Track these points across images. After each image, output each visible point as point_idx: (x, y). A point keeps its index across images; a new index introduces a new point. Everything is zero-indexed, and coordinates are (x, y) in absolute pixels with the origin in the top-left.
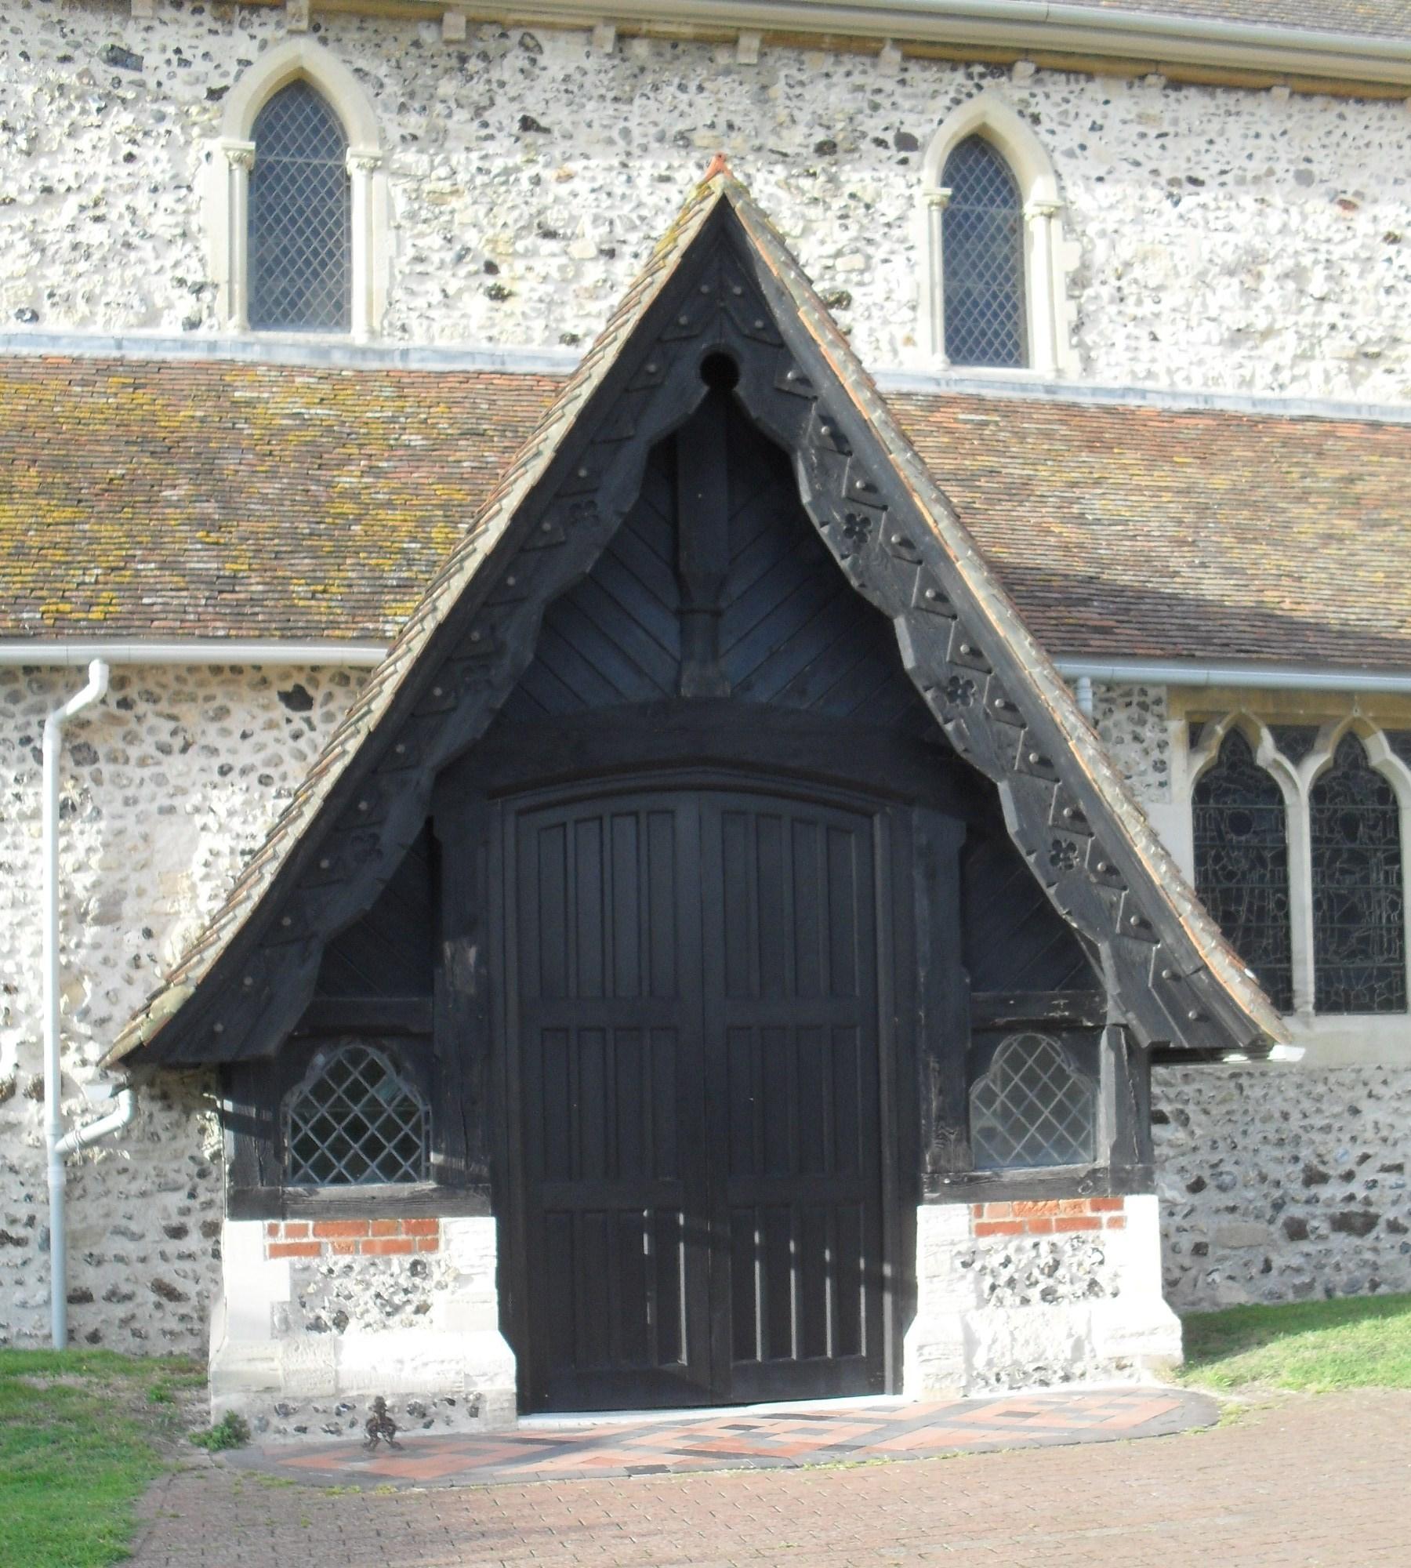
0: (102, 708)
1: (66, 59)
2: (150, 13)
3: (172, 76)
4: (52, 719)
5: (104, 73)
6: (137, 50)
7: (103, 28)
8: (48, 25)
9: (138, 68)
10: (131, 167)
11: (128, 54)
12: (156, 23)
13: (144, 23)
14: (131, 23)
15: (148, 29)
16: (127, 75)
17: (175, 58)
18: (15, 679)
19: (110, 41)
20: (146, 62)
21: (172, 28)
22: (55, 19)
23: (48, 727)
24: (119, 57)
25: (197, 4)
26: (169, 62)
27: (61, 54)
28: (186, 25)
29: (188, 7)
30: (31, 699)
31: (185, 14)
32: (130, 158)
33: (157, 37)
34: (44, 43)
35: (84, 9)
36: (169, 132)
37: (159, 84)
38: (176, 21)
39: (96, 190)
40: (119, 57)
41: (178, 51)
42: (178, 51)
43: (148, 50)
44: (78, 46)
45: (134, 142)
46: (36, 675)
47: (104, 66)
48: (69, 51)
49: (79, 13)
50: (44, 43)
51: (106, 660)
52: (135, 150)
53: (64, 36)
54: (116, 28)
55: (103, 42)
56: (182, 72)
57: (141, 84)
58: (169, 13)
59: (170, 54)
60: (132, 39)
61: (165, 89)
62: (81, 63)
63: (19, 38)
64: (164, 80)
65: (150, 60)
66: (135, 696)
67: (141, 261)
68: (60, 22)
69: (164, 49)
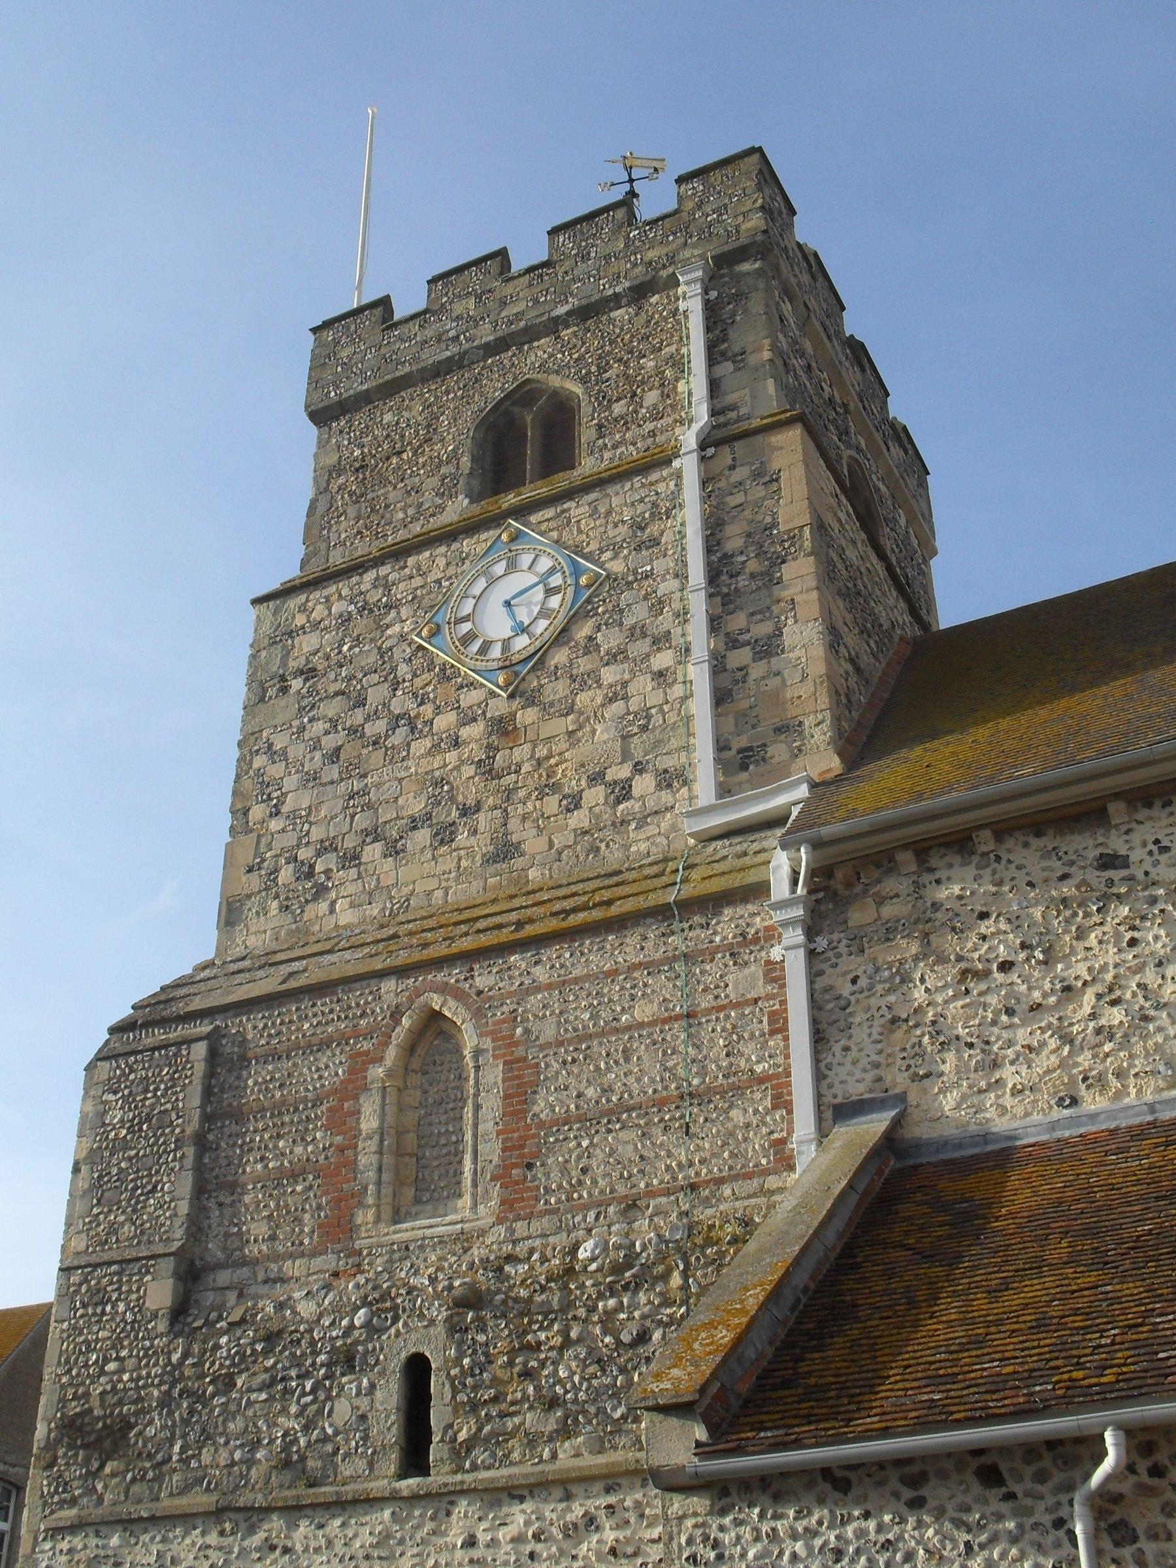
0: (1132, 1479)
1: (1064, 877)
2: (1127, 819)
3: (1156, 863)
4: (1078, 1497)
5: (1096, 878)
6: (1122, 852)
7: (1090, 843)
8: (1046, 855)
9: (1128, 867)
10: (1135, 950)
11: (1115, 856)
12: (1134, 825)
13: (1124, 828)
14: (1113, 831)
15: (1127, 832)
16: (1116, 875)
17: (1155, 848)
18: (1040, 1457)
19: (1097, 852)
20: (1131, 859)
21: (1149, 824)
22: (1050, 848)
23: (1077, 1507)
24: (1109, 862)
25: (1166, 798)
26: (1151, 853)
27: (1059, 874)
28: (1159, 819)
29: (1158, 803)
30: (1058, 1477)
31: (1156, 811)
32: (1133, 942)
33: (1136, 838)
35: (1072, 833)
36: (1162, 911)
37: (1147, 874)
38: (1150, 818)
39: (1109, 977)
40: (1109, 862)
41: (1157, 842)
42: (1157, 842)
43: (1131, 849)
44: (1072, 863)
45: (1133, 928)
46: (1060, 1449)
47: (1098, 873)
48: (1066, 870)
49: (1069, 838)
51: (1119, 1427)
52: (1136, 934)
53: (1060, 859)
54: (1101, 840)
55: (1093, 854)
56: (1164, 858)
57: (1131, 878)
58: (1142, 814)
59: (1151, 847)
60: (1117, 844)
61: (1153, 876)
62: (1078, 876)
63: (1024, 871)
64: (1149, 869)
65: (1134, 857)
66: (1167, 1462)
67: (1160, 1029)
68: (1054, 849)
69: (1144, 844)
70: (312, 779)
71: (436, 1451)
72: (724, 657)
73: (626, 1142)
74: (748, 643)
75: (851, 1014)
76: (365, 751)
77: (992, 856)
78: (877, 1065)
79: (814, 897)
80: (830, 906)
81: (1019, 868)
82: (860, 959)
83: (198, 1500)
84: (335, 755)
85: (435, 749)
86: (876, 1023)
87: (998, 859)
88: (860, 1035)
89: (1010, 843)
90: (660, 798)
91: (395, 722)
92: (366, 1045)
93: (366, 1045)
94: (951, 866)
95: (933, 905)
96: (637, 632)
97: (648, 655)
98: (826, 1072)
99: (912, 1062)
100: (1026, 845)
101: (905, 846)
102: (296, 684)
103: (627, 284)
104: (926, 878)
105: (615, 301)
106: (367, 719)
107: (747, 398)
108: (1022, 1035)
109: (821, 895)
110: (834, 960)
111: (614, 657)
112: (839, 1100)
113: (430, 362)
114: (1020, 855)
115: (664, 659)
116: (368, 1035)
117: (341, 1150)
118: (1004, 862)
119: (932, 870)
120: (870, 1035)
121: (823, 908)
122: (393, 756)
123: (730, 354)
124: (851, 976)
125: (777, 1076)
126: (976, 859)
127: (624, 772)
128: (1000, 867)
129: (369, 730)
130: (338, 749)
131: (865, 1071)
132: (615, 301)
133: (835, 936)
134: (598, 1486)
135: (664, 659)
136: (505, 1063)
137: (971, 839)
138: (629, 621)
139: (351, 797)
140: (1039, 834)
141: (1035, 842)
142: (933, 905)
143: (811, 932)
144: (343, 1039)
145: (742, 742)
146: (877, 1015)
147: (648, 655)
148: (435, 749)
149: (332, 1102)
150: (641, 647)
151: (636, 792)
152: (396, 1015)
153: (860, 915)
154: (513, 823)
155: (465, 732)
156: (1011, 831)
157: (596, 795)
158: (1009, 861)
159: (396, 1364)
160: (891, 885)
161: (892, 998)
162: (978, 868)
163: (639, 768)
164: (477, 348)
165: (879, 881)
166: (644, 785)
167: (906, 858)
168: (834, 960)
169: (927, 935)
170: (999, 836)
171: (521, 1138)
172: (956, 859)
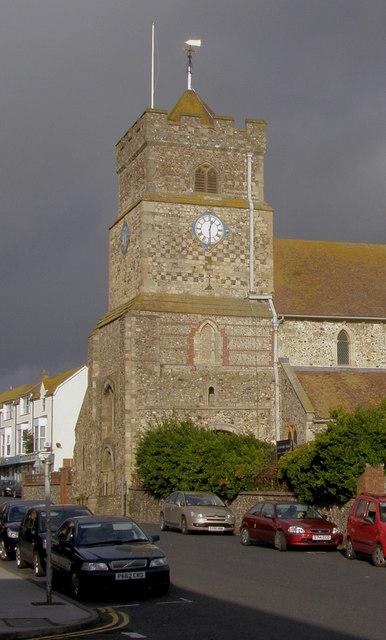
96: (237, 248)
111: (232, 252)
115: (243, 257)
122: (184, 257)
135: (243, 257)
150: (238, 252)
155: (200, 258)
157: (228, 282)
166: (238, 283)
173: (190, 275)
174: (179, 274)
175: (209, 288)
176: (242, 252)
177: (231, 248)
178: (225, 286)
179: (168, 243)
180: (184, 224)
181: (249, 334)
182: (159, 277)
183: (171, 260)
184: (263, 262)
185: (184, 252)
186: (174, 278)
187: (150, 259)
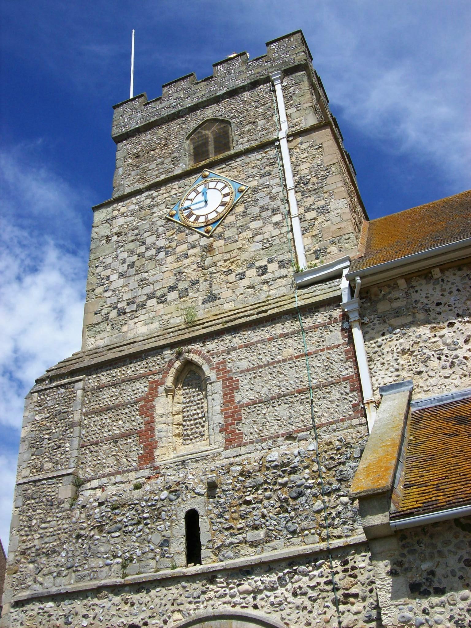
8: (463, 278)
34: (464, 284)
50: (464, 284)
63: (455, 285)
68: (467, 275)
70: (122, 275)
71: (204, 553)
72: (304, 215)
73: (282, 410)
74: (313, 209)
75: (383, 349)
76: (147, 262)
77: (440, 280)
78: (397, 370)
79: (362, 301)
80: (369, 304)
81: (453, 284)
82: (385, 325)
83: (87, 584)
84: (132, 265)
85: (178, 260)
86: (395, 351)
87: (443, 281)
88: (389, 357)
89: (447, 273)
90: (280, 272)
91: (159, 250)
92: (157, 377)
93: (157, 377)
94: (421, 284)
95: (416, 301)
96: (263, 208)
97: (270, 216)
98: (374, 374)
99: (414, 367)
100: (455, 274)
101: (402, 277)
102: (115, 238)
103: (249, 82)
104: (411, 290)
105: (243, 89)
106: (147, 249)
107: (303, 121)
108: (461, 353)
109: (364, 300)
110: (372, 327)
111: (254, 219)
112: (382, 385)
113: (165, 115)
114: (452, 278)
115: (277, 218)
116: (158, 373)
117: (147, 423)
118: (445, 282)
119: (413, 287)
120: (393, 357)
121: (365, 305)
122: (160, 263)
123: (294, 105)
124: (381, 333)
125: (352, 377)
126: (432, 281)
127: (264, 262)
128: (444, 285)
129: (148, 254)
130: (134, 263)
131: (392, 372)
132: (243, 89)
133: (372, 317)
134: (284, 564)
136: (223, 380)
137: (431, 273)
138: (261, 204)
139: (142, 281)
140: (460, 269)
141: (459, 273)
142: (416, 301)
143: (362, 316)
144: (145, 376)
145: (317, 247)
146: (395, 348)
147: (270, 216)
148: (178, 260)
149: (142, 403)
151: (269, 270)
152: (171, 364)
153: (382, 307)
154: (214, 287)
155: (191, 252)
156: (447, 269)
158: (448, 281)
159: (182, 515)
160: (395, 294)
161: (401, 341)
162: (434, 284)
163: (270, 261)
164: (185, 109)
165: (390, 293)
167: (402, 283)
168: (372, 327)
169: (414, 313)
170: (442, 271)
171: (233, 412)
172: (424, 282)
173: (172, 289)
174: (150, 297)
175: (212, 298)
176: (275, 211)
177: (255, 210)
178: (245, 282)
179: (131, 252)
180: (159, 214)
181: (289, 352)
182: (114, 314)
183: (138, 277)
184: (324, 211)
185: (162, 255)
186: (142, 306)
187: (99, 290)
